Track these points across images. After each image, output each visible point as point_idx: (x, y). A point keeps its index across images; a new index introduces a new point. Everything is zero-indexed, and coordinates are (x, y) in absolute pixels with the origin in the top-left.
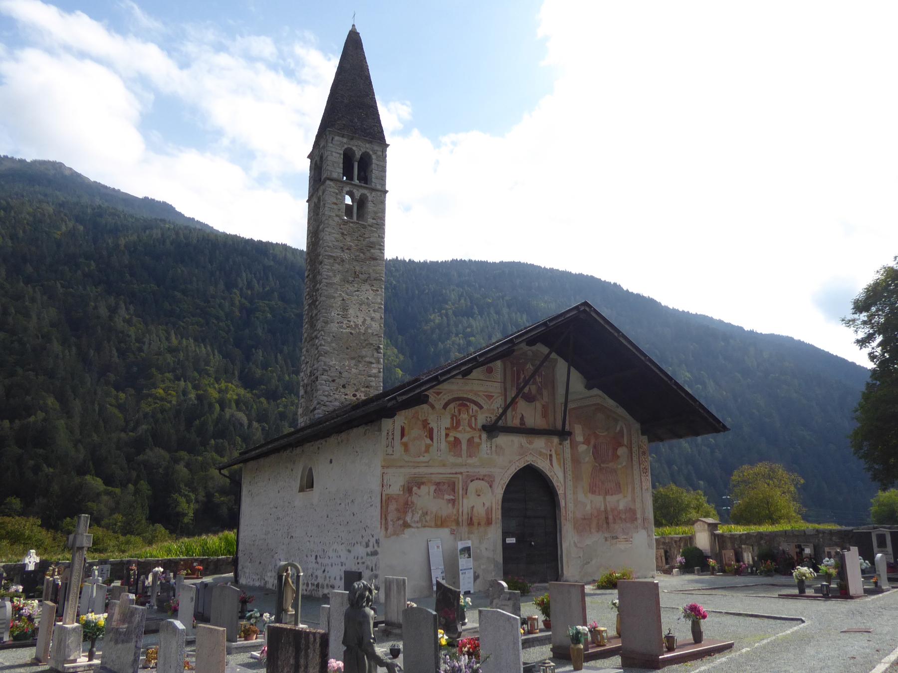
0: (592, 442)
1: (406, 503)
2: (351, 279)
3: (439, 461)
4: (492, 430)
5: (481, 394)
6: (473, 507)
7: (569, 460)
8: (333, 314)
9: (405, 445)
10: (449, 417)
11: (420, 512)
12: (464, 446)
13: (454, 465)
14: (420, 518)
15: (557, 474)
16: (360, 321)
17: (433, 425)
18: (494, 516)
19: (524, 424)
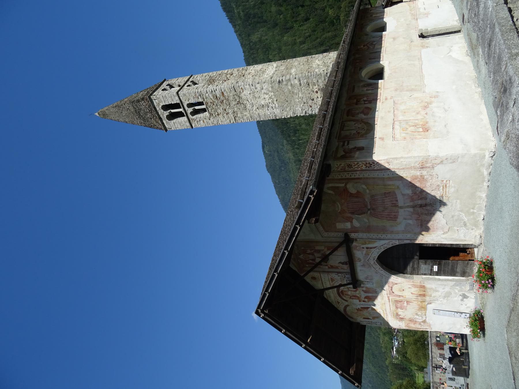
0: (350, 215)
2: (243, 106)
4: (355, 283)
6: (412, 293)
7: (368, 235)
8: (269, 113)
9: (374, 318)
10: (351, 300)
12: (370, 295)
15: (382, 244)
16: (267, 96)
17: (359, 307)
18: (418, 284)
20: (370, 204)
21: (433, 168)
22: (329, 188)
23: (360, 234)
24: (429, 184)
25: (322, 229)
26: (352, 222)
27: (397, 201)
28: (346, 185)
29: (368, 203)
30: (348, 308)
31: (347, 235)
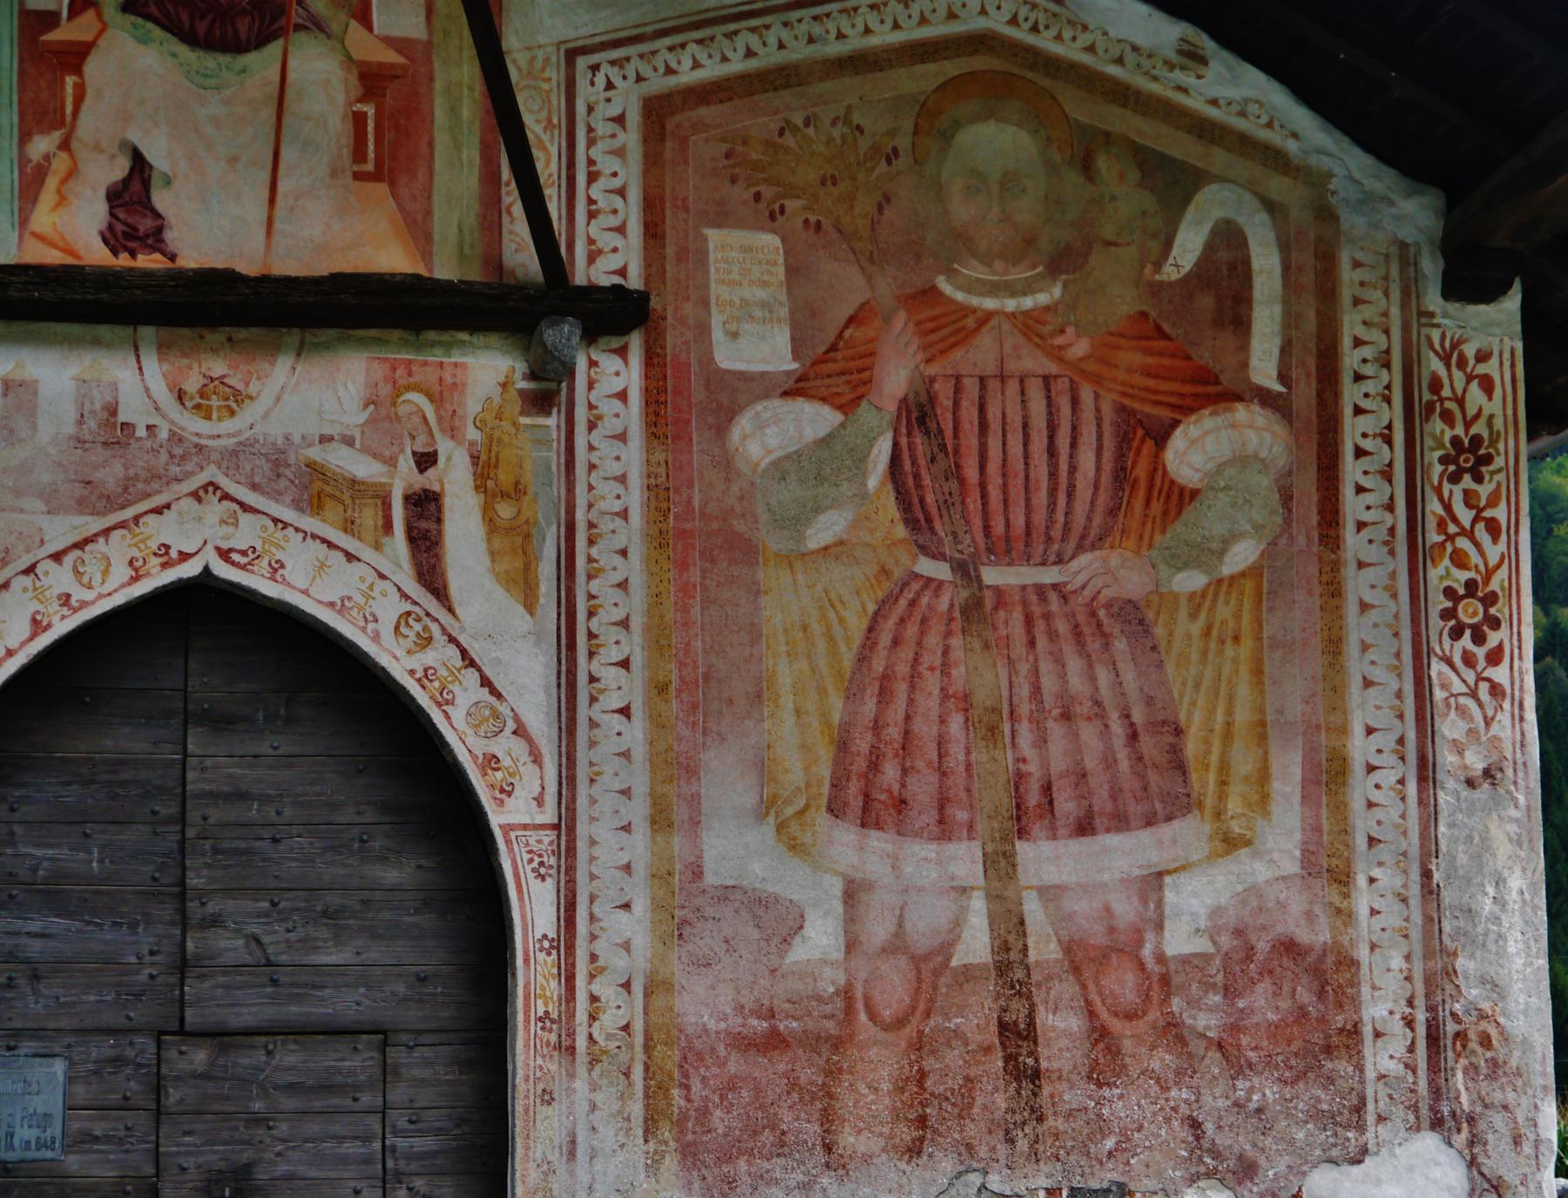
0: (896, 377)
19: (155, 240)
20: (1040, 590)
21: (1437, 1124)
22: (1228, 238)
23: (634, 455)
24: (1267, 1091)
25: (687, 77)
26: (797, 388)
27: (1084, 828)
28: (1265, 398)
29: (1050, 575)
31: (615, 314)
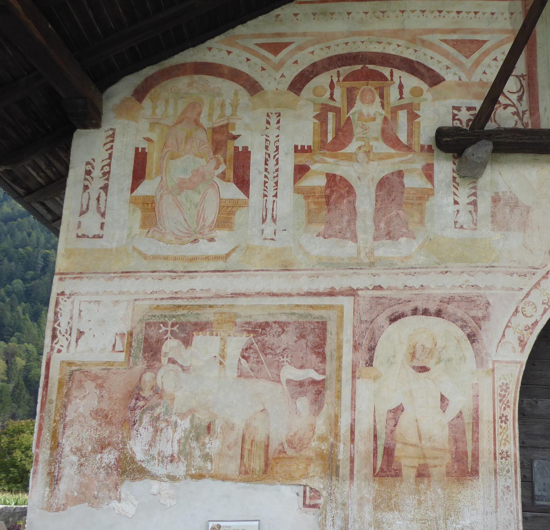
1: (135, 393)
3: (268, 250)
5: (435, 38)
11: (185, 424)
12: (365, 201)
13: (332, 264)
14: (183, 443)
30: (228, 88)
